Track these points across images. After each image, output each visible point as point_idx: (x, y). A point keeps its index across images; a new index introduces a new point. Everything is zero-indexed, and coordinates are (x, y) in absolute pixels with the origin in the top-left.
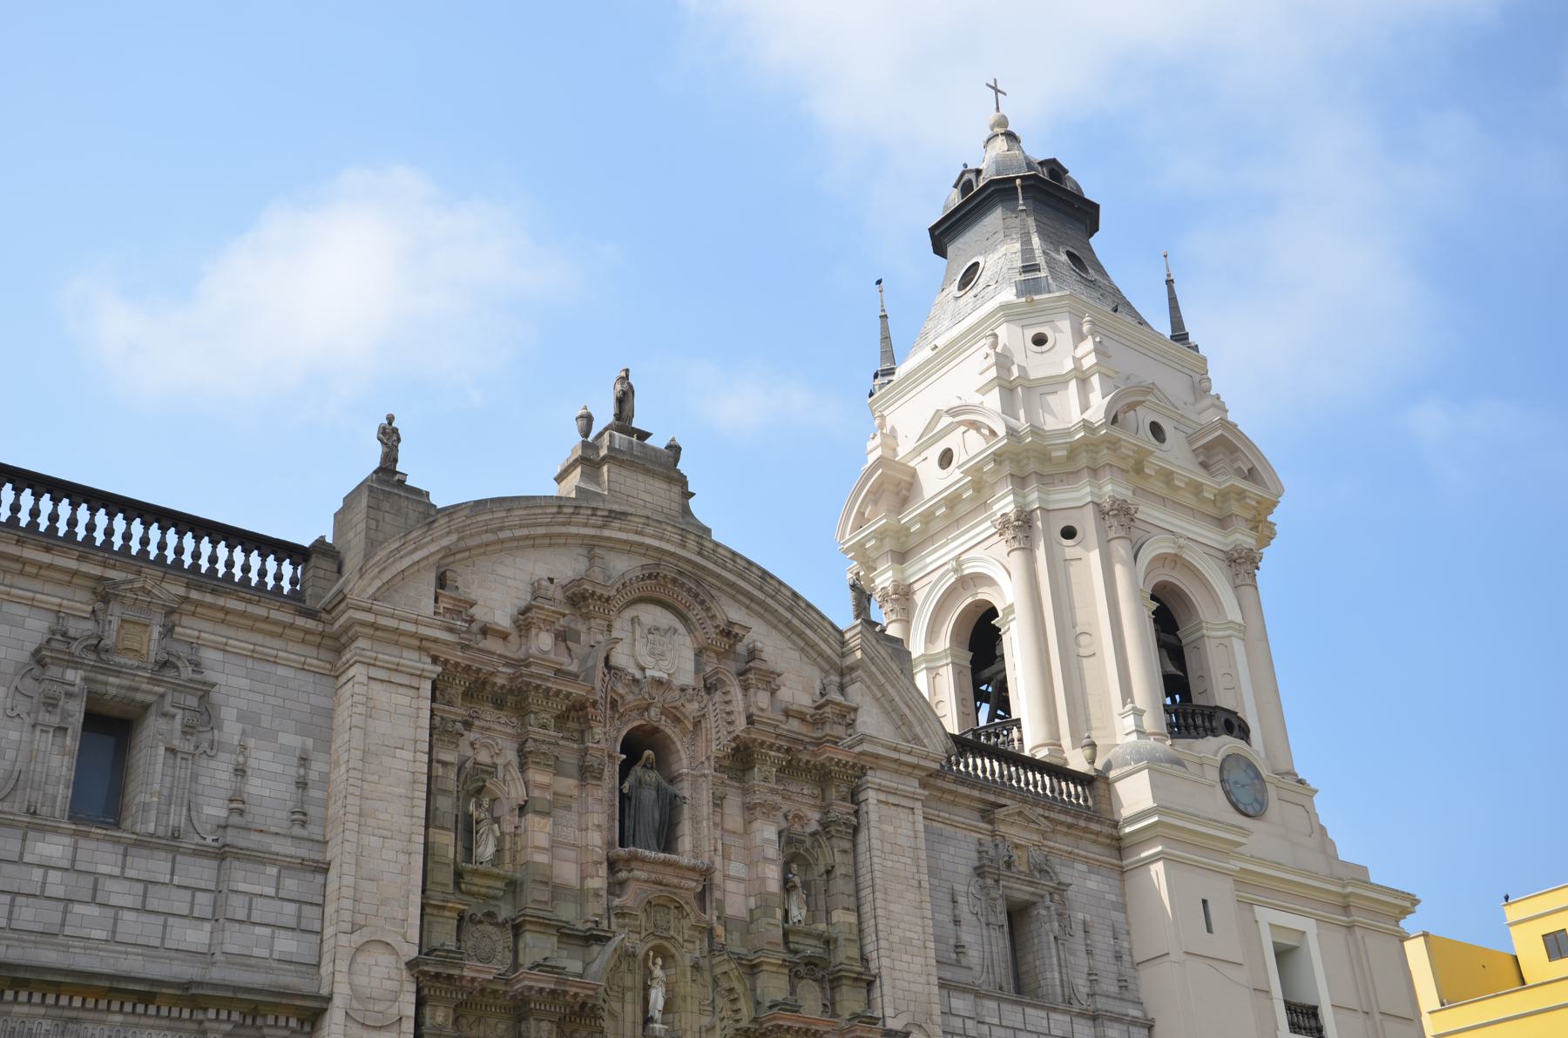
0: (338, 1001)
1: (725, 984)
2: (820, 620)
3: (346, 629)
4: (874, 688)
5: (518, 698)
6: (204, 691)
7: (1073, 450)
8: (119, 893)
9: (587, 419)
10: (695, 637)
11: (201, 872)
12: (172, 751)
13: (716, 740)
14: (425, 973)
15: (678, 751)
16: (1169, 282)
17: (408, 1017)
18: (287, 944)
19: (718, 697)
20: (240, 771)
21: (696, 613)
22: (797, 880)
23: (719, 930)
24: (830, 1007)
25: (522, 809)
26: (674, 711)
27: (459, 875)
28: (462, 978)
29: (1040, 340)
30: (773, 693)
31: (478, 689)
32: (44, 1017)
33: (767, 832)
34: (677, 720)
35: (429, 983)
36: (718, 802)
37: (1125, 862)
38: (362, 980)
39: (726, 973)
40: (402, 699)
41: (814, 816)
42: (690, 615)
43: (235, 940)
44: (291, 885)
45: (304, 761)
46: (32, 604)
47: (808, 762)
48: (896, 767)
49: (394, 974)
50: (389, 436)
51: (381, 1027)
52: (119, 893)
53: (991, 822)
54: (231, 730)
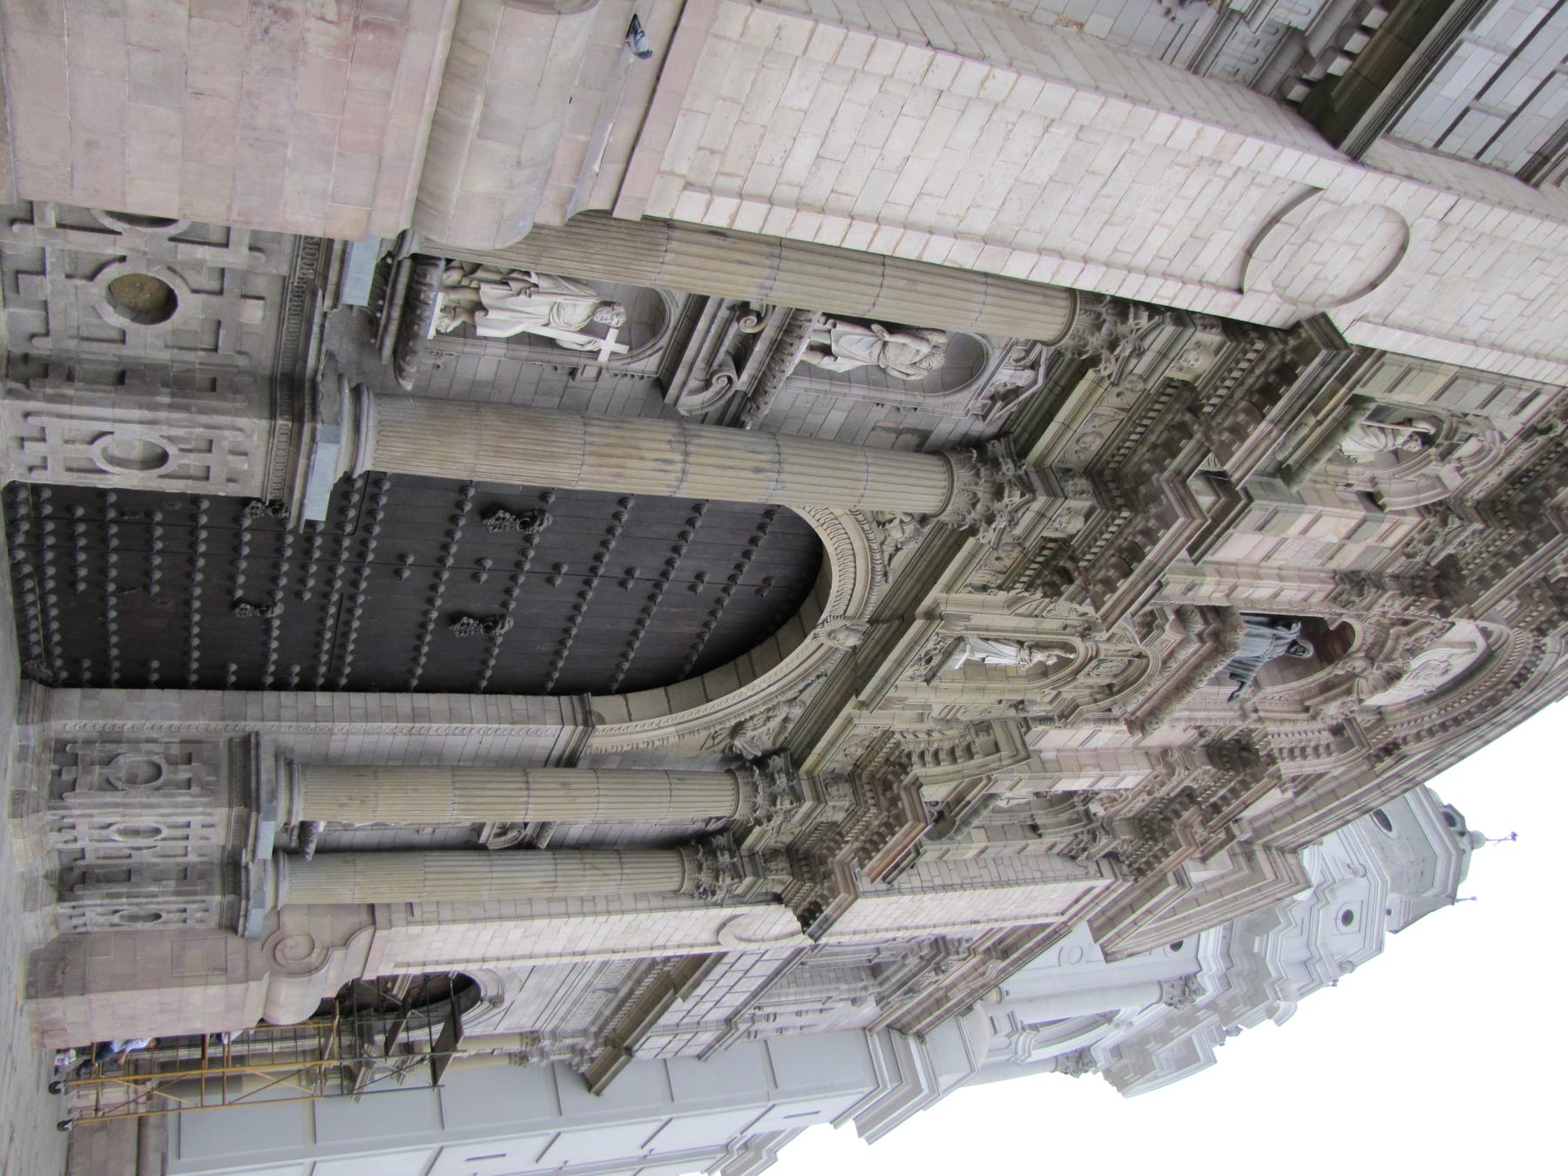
0: (1349, 176)
1: (980, 741)
2: (1323, 830)
4: (1221, 883)
5: (1515, 509)
7: (1257, 961)
10: (1400, 710)
14: (1304, 353)
15: (1285, 682)
17: (1234, 306)
19: (1326, 737)
21: (1432, 715)
25: (1372, 499)
26: (1344, 687)
28: (1257, 414)
29: (1348, 918)
34: (1326, 687)
35: (1273, 354)
37: (876, 1037)
39: (997, 749)
42: (1433, 709)
47: (1179, 816)
48: (1123, 903)
49: (1317, 289)
51: (1249, 252)
53: (988, 951)
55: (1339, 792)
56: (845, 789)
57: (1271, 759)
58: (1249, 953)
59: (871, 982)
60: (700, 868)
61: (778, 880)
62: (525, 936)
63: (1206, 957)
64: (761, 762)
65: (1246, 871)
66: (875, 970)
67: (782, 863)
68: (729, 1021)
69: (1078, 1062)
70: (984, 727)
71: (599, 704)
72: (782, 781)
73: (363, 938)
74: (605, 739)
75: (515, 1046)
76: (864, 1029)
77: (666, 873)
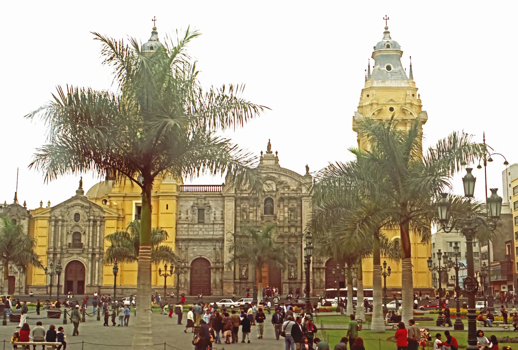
6: (210, 206)
8: (203, 230)
9: (262, 153)
11: (211, 226)
13: (278, 197)
16: (411, 66)
18: (221, 233)
20: (215, 214)
22: (292, 214)
23: (278, 223)
24: (296, 230)
27: (241, 222)
30: (289, 188)
31: (243, 199)
33: (286, 209)
36: (279, 206)
38: (227, 236)
40: (231, 203)
41: (296, 204)
43: (215, 233)
44: (221, 226)
45: (222, 212)
46: (191, 200)
52: (203, 230)
54: (214, 210)
61: (299, 239)
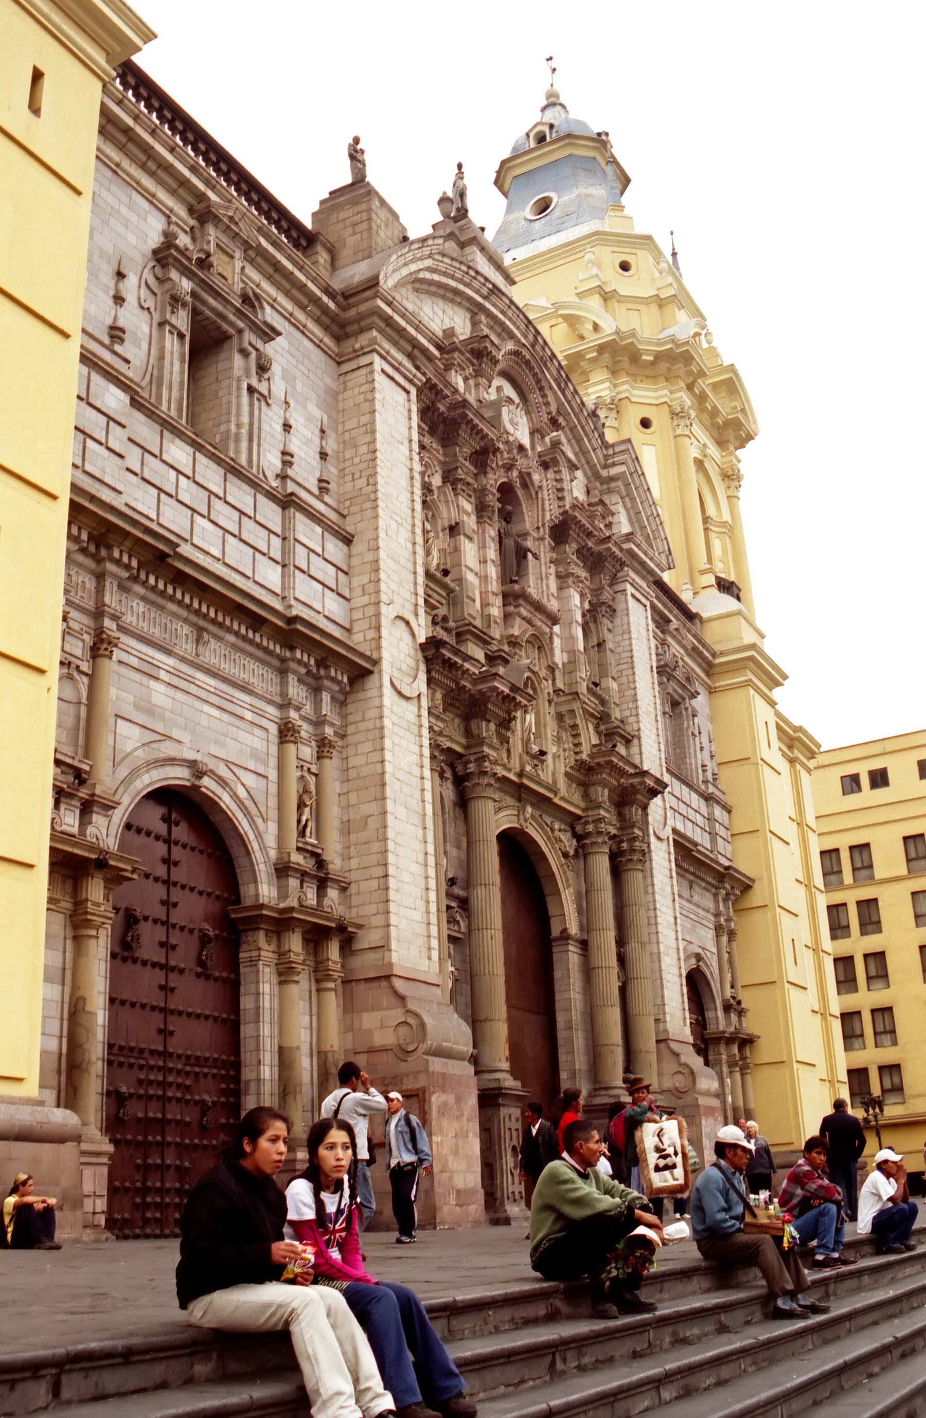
1: (568, 721)
3: (361, 317)
7: (659, 357)
11: (270, 513)
12: (251, 390)
19: (550, 474)
29: (625, 266)
32: (185, 620)
42: (531, 397)
50: (355, 155)
55: (572, 425)
56: (592, 790)
57: (565, 513)
58: (653, 363)
59: (682, 706)
60: (630, 860)
61: (635, 813)
62: (668, 955)
63: (657, 398)
64: (578, 837)
65: (620, 483)
66: (675, 704)
67: (626, 811)
68: (708, 798)
69: (731, 477)
70: (560, 717)
71: (555, 932)
72: (590, 828)
73: (673, 1045)
74: (573, 929)
75: (725, 939)
76: (710, 693)
77: (634, 879)
